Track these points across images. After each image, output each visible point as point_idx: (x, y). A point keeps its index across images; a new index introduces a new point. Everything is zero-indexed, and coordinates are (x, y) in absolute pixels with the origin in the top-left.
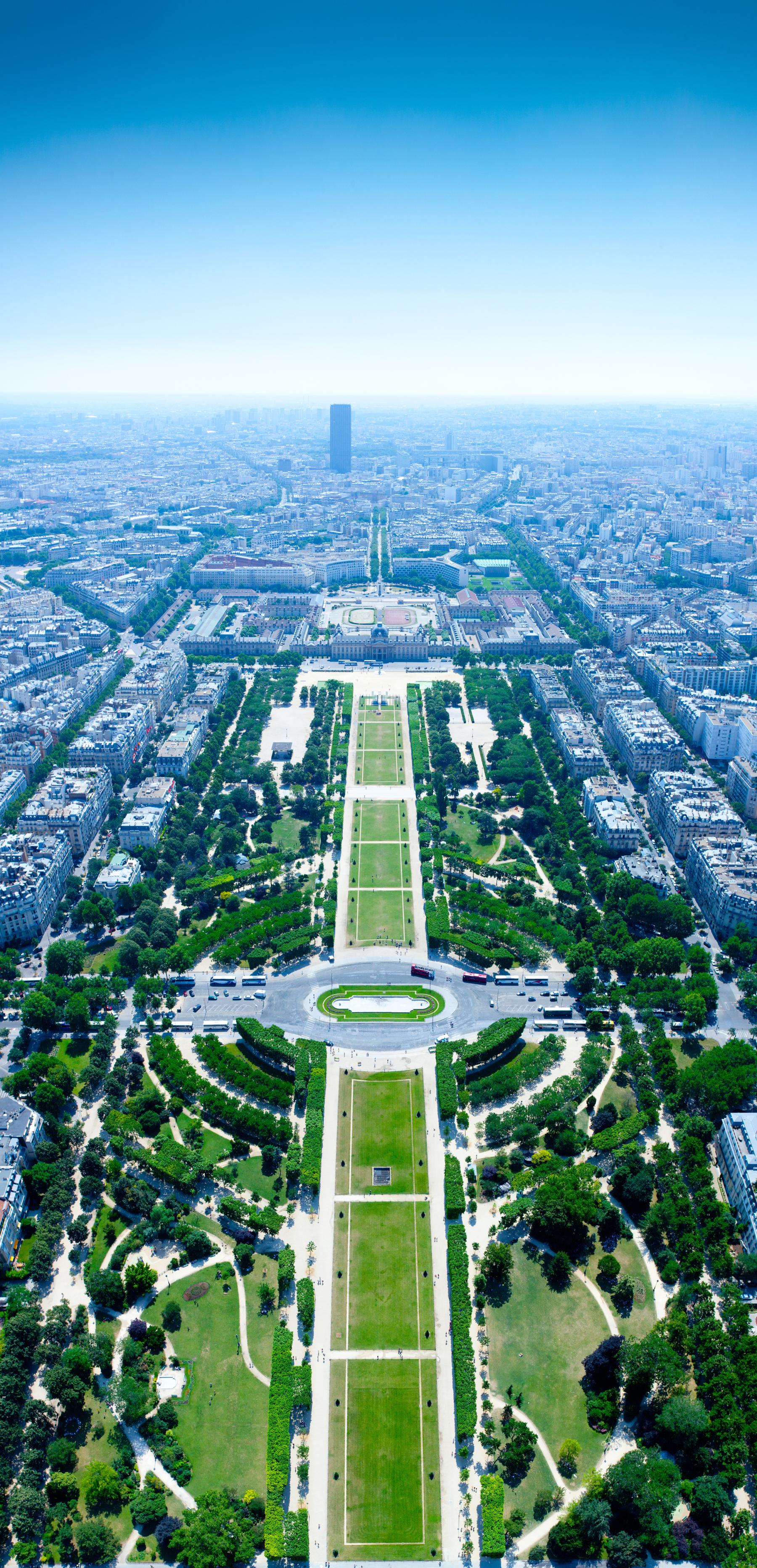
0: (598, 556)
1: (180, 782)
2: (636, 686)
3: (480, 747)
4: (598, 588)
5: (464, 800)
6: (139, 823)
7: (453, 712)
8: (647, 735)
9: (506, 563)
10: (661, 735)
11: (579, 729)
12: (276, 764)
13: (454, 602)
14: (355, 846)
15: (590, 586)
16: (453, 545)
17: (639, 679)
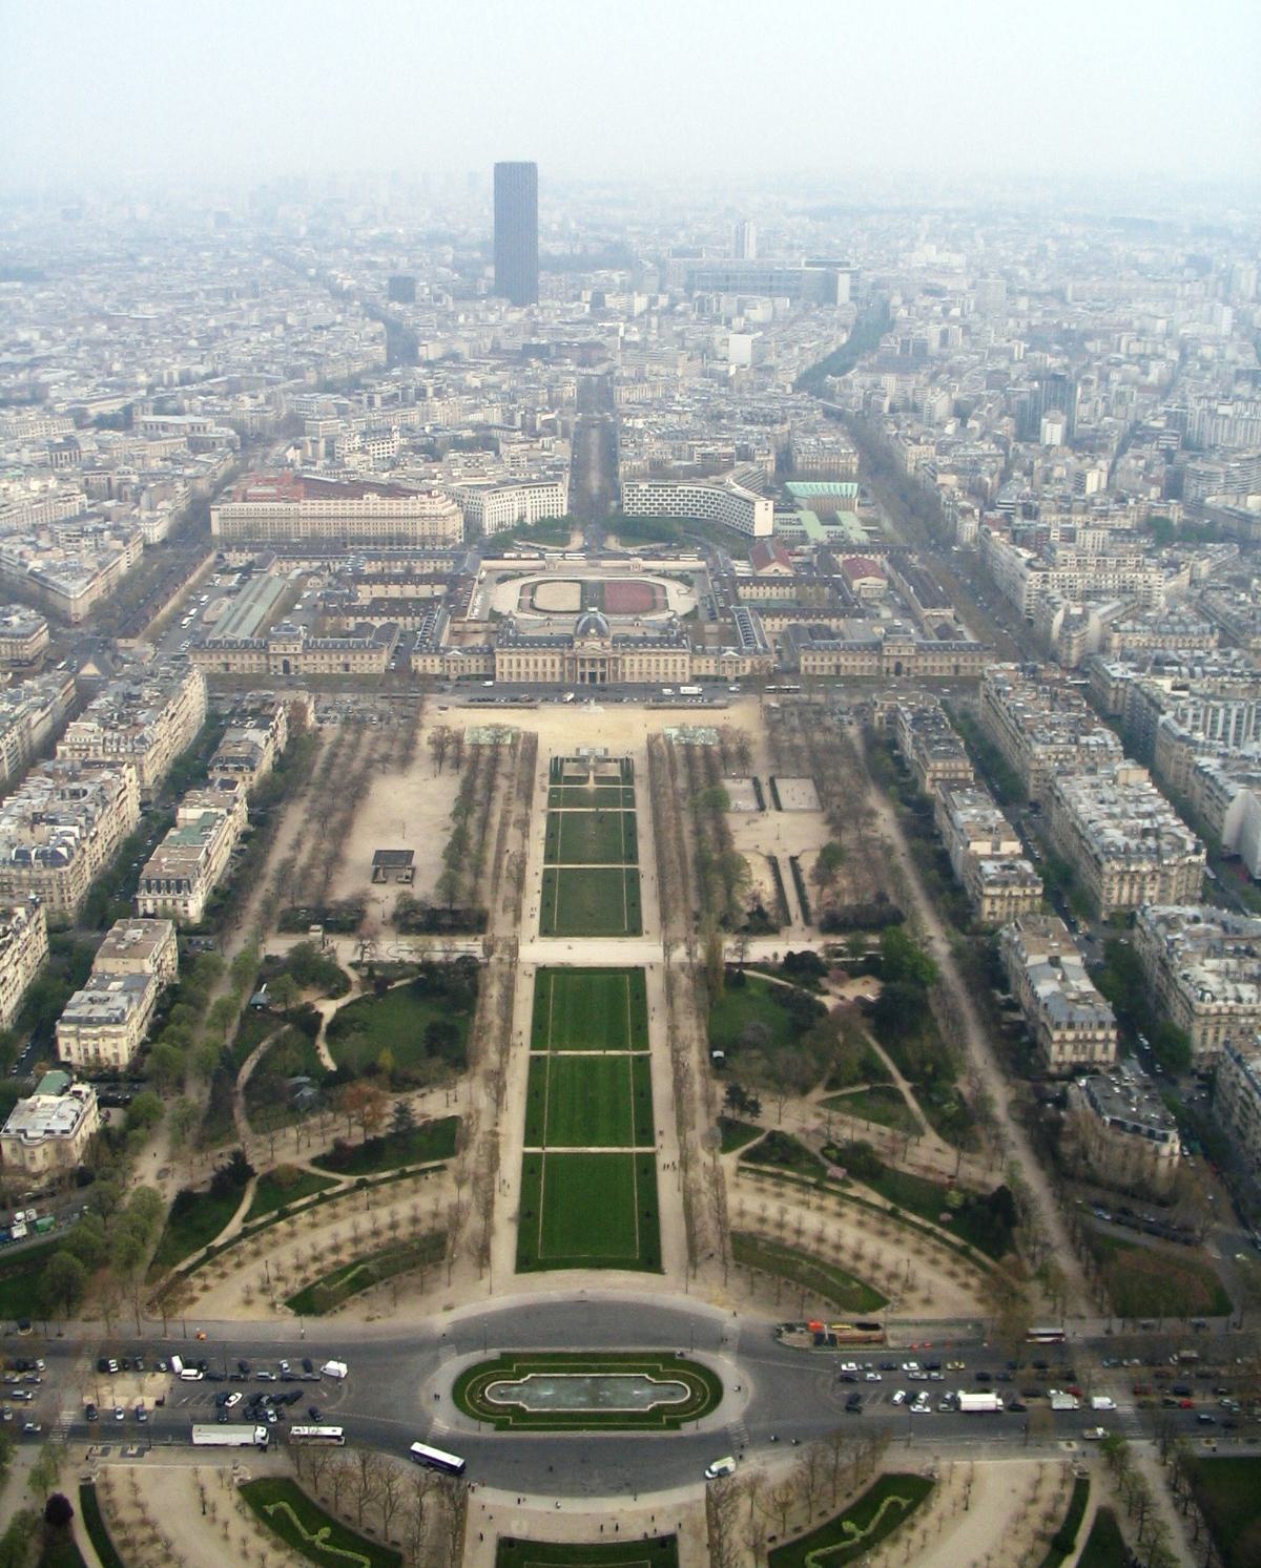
0: (1038, 477)
1: (185, 931)
2: (1109, 738)
3: (793, 860)
4: (1038, 542)
5: (761, 967)
6: (100, 1012)
7: (738, 791)
8: (1129, 833)
9: (852, 488)
10: (1157, 834)
11: (992, 823)
12: (379, 891)
13: (742, 568)
14: (539, 1058)
15: (1019, 538)
16: (745, 455)
17: (1112, 720)
